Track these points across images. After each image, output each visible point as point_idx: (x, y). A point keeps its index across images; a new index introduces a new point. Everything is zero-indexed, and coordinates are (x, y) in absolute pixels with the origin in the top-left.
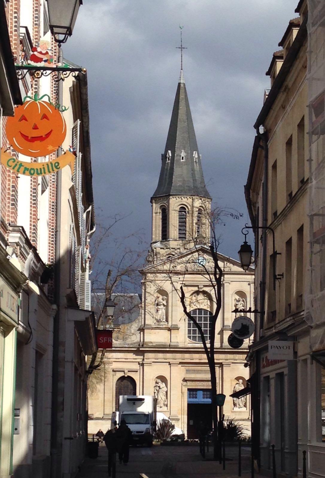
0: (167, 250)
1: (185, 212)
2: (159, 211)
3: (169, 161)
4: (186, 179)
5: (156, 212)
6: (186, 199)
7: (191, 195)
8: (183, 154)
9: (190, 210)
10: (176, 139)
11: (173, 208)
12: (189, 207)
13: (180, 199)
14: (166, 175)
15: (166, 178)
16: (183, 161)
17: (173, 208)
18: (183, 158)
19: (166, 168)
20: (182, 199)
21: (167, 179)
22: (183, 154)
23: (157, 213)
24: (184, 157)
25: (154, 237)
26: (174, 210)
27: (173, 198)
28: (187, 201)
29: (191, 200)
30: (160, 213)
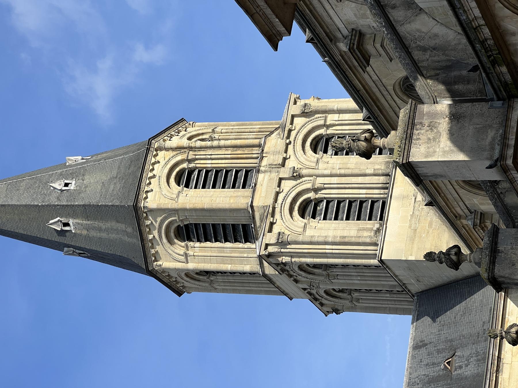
0: (277, 216)
1: (191, 172)
2: (179, 247)
3: (71, 222)
4: (114, 173)
5: (183, 258)
6: (156, 166)
7: (148, 150)
8: (58, 185)
9: (184, 156)
10: (26, 206)
11: (172, 199)
12: (179, 158)
13: (152, 181)
14: (100, 230)
15: (107, 230)
16: (74, 182)
17: (172, 199)
18: (66, 185)
19: (85, 232)
20: (154, 176)
21: (108, 225)
22: (58, 185)
23: (186, 255)
24: (66, 181)
25: (247, 268)
26: (178, 196)
27: (146, 198)
28: (162, 162)
29: (161, 154)
30: (187, 247)
